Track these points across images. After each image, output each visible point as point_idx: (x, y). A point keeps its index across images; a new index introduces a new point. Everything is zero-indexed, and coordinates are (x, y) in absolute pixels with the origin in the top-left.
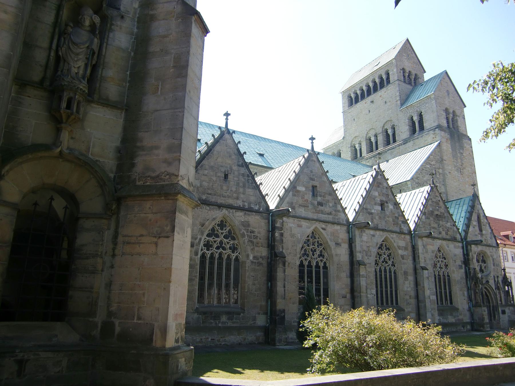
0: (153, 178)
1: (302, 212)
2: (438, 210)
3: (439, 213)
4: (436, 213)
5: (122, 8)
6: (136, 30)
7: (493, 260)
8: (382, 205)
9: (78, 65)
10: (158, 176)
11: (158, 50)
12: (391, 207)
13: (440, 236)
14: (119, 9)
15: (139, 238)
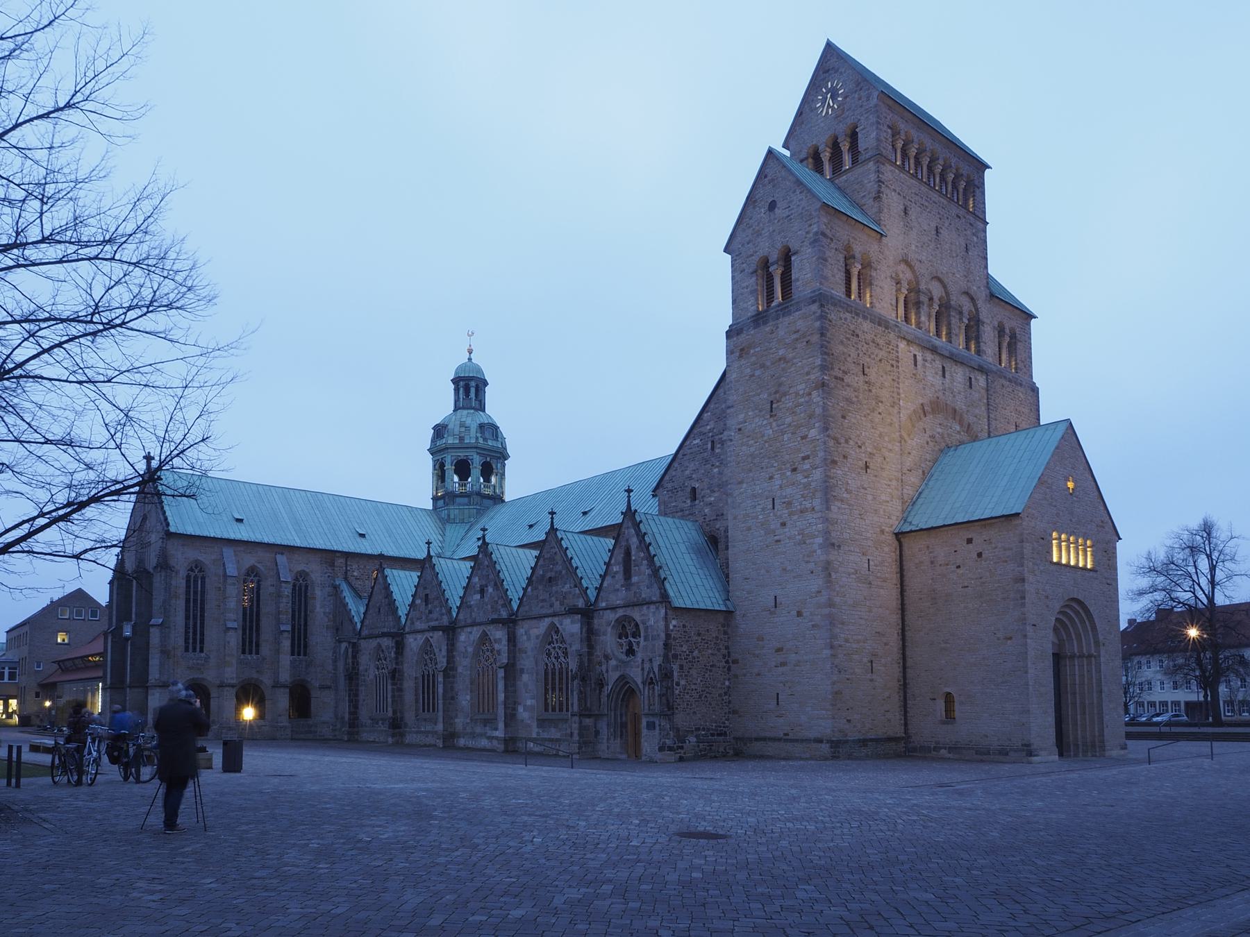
1: (419, 625)
2: (551, 570)
3: (553, 574)
4: (549, 575)
7: (646, 629)
8: (482, 591)
12: (490, 590)
13: (550, 611)
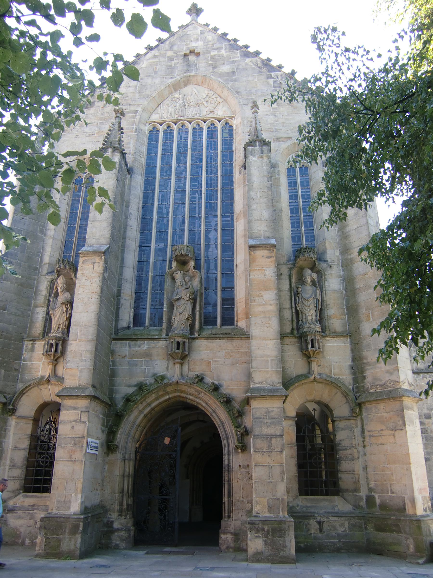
0: (381, 386)
5: (329, 260)
6: (342, 273)
9: (310, 314)
10: (384, 384)
11: (363, 286)
14: (327, 261)
15: (381, 432)
